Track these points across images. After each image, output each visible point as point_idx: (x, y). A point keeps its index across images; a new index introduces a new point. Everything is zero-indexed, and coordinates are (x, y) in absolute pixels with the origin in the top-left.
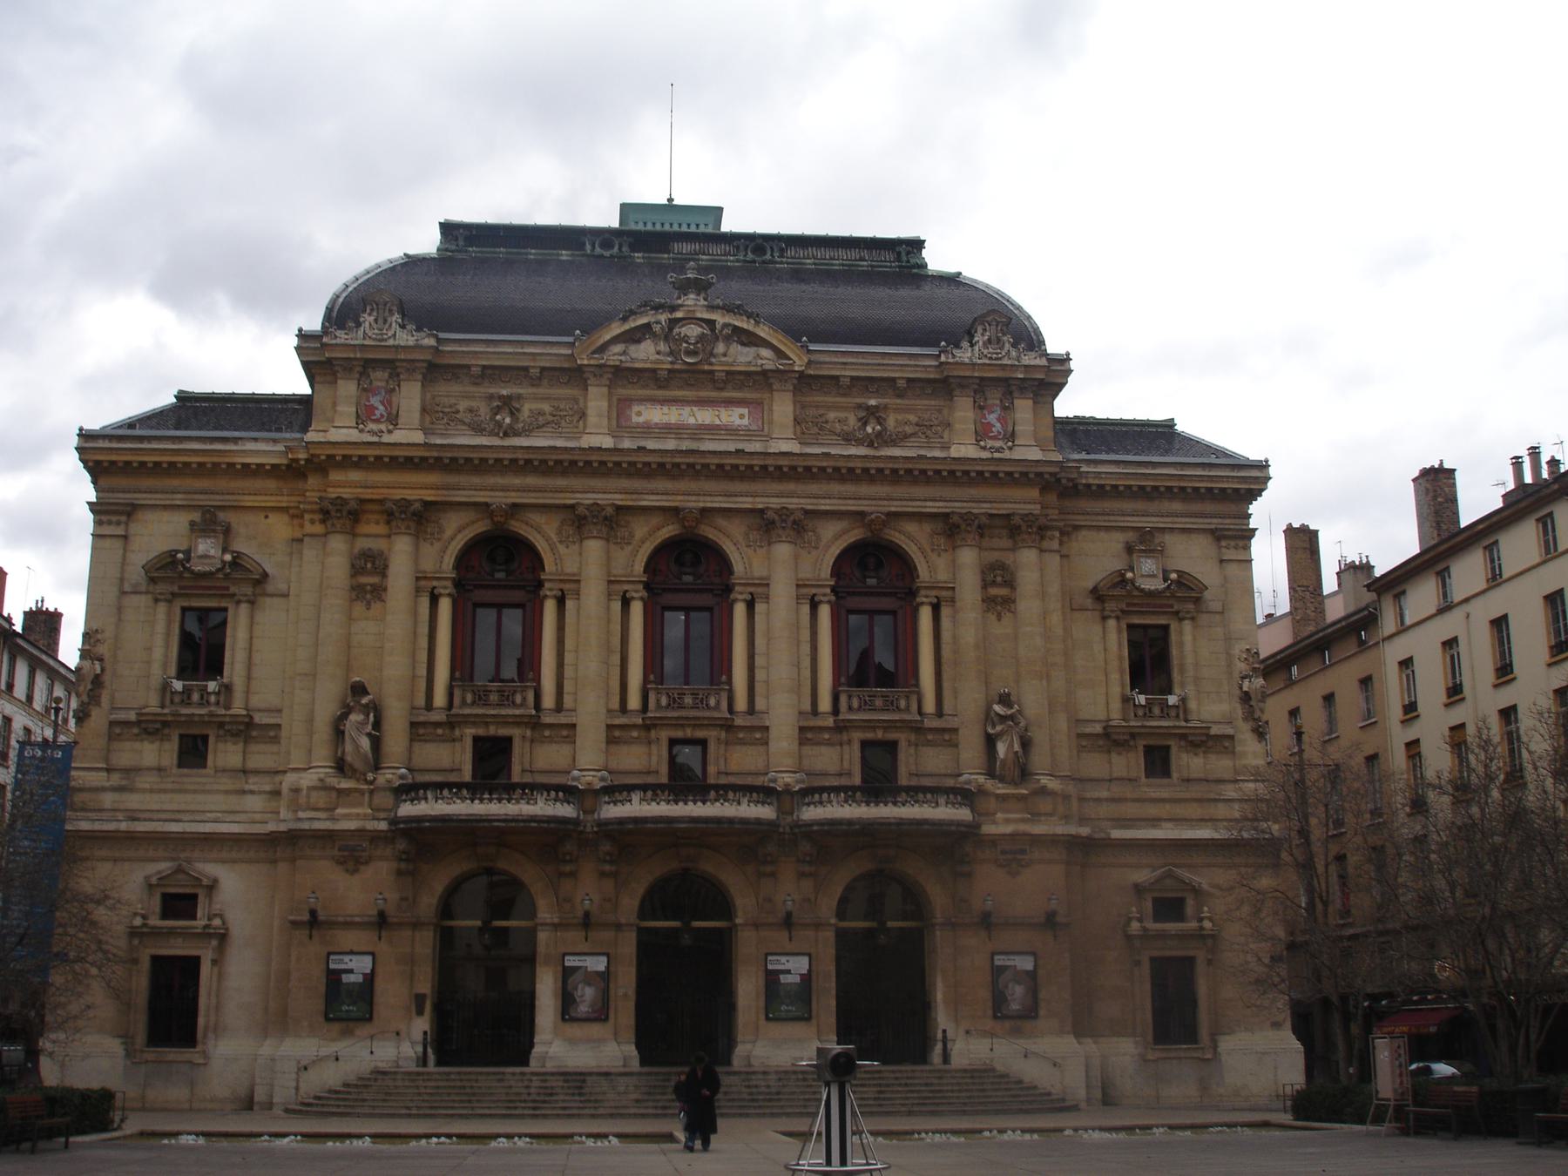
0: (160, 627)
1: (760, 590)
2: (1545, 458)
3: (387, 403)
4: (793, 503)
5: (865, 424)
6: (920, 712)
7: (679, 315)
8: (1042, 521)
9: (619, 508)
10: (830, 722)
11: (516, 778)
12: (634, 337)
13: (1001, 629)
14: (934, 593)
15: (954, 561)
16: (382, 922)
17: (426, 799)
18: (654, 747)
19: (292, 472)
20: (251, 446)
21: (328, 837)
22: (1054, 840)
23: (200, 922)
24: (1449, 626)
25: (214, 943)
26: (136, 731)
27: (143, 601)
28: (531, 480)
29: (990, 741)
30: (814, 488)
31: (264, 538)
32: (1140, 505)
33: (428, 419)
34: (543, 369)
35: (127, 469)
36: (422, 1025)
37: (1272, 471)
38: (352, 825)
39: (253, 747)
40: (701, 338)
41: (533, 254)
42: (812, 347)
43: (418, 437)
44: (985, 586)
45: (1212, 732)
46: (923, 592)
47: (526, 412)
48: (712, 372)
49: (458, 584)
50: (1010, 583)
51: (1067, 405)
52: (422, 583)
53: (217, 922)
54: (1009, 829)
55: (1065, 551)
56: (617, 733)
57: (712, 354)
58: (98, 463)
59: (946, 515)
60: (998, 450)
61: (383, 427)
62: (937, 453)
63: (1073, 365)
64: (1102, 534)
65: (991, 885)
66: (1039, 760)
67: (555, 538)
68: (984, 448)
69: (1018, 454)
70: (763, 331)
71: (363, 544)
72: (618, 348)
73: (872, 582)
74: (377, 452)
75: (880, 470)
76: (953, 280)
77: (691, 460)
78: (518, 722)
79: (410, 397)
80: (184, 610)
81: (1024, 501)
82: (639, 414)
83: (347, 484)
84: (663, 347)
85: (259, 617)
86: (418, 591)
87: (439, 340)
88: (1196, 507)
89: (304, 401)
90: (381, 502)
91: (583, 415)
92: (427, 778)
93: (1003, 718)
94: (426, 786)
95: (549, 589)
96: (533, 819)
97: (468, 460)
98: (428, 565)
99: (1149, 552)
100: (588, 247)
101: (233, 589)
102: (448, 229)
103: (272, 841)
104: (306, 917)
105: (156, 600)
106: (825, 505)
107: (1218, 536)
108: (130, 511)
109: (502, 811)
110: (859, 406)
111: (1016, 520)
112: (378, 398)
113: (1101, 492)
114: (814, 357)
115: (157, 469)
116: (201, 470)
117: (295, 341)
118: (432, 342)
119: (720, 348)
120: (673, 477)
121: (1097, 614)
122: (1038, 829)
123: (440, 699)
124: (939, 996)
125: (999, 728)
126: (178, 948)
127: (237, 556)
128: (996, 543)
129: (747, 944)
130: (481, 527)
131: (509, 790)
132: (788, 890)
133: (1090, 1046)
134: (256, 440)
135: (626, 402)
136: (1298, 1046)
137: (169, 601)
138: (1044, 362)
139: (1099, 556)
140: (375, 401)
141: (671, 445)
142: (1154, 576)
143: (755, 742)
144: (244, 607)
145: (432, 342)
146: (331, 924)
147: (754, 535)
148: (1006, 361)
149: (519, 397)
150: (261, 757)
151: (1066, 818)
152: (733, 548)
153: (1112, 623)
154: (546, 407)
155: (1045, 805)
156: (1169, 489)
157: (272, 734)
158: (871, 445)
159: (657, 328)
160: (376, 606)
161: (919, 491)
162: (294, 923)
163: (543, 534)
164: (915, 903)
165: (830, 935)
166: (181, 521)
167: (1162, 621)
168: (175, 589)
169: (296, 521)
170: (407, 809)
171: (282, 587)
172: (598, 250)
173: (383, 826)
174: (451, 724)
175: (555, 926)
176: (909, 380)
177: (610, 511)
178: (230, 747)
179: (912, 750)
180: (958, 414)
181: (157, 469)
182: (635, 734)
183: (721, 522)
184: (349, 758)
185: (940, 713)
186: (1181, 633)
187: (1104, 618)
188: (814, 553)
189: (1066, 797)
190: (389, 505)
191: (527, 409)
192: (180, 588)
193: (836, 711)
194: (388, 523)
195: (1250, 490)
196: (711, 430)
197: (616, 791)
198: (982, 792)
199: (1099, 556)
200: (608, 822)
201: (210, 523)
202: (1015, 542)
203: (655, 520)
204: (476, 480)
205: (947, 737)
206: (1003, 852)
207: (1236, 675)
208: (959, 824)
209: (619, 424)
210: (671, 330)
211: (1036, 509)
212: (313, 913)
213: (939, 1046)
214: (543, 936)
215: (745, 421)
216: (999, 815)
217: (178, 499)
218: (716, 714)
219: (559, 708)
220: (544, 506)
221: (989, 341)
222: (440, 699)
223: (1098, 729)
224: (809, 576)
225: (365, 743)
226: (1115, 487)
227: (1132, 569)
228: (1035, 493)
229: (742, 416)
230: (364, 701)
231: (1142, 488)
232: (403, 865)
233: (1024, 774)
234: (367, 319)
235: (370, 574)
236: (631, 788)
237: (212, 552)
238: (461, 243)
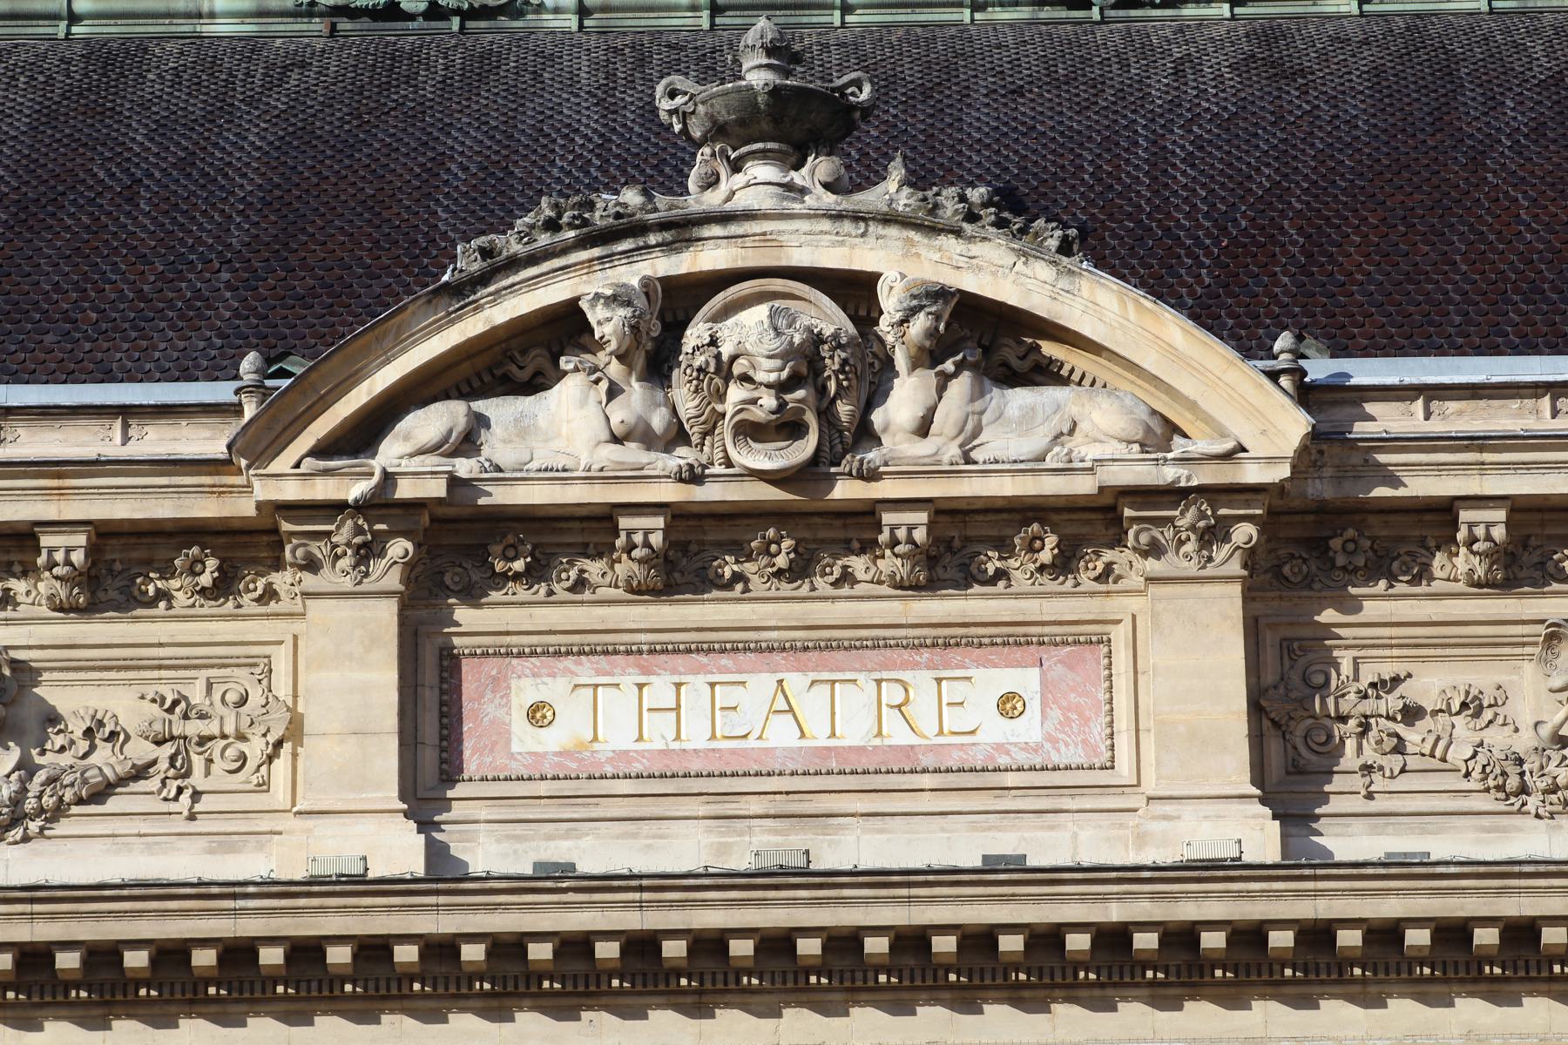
12: (524, 360)
72: (434, 421)
119: (905, 398)
141: (685, 848)
159: (607, 323)
196: (879, 776)
215: (1028, 729)
229: (1009, 705)
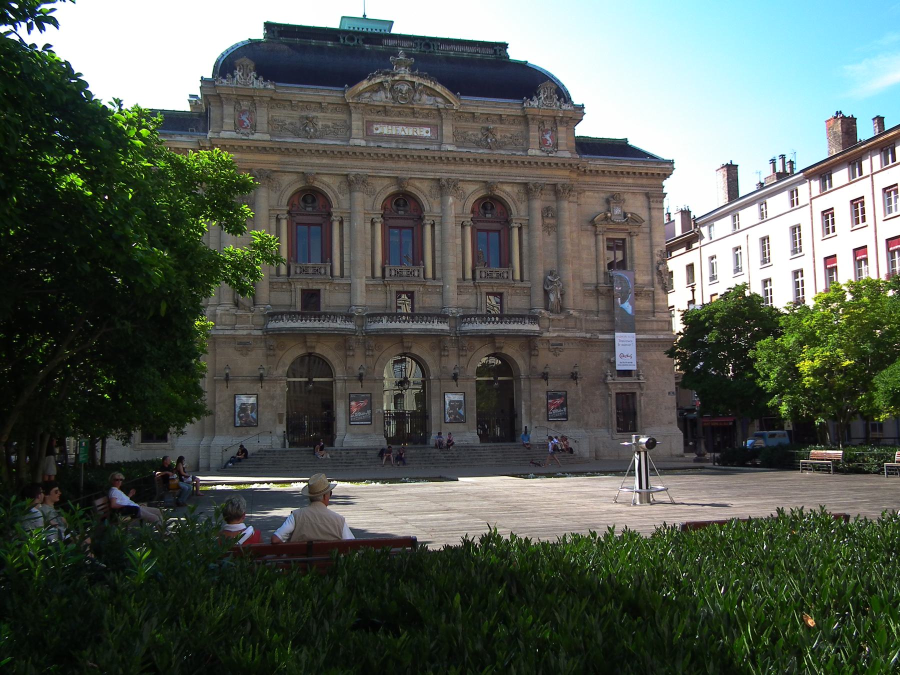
2: (787, 160)
3: (250, 119)
4: (454, 176)
7: (397, 78)
11: (322, 310)
21: (234, 337)
22: (575, 339)
24: (738, 240)
28: (325, 161)
29: (546, 293)
32: (614, 180)
36: (281, 429)
38: (245, 332)
41: (314, 42)
43: (267, 137)
51: (581, 130)
54: (555, 335)
63: (585, 110)
66: (569, 302)
72: (367, 95)
76: (523, 66)
77: (405, 153)
79: (262, 116)
81: (561, 176)
82: (377, 129)
88: (639, 181)
91: (349, 128)
96: (336, 329)
100: (342, 40)
102: (268, 26)
117: (200, 84)
118: (273, 87)
119: (417, 96)
122: (568, 335)
124: (523, 411)
125: (550, 287)
131: (319, 316)
135: (369, 125)
136: (680, 433)
139: (593, 203)
151: (581, 330)
154: (330, 124)
155: (571, 323)
159: (386, 85)
161: (514, 171)
162: (215, 380)
170: (273, 325)
172: (347, 42)
173: (260, 333)
175: (345, 380)
180: (531, 134)
188: (463, 201)
191: (320, 123)
193: (474, 278)
197: (374, 316)
208: (534, 331)
209: (368, 134)
211: (567, 181)
214: (339, 385)
215: (429, 135)
220: (331, 174)
228: (567, 173)
229: (427, 132)
232: (272, 352)
233: (562, 309)
234: (238, 73)
236: (381, 315)
238: (276, 34)
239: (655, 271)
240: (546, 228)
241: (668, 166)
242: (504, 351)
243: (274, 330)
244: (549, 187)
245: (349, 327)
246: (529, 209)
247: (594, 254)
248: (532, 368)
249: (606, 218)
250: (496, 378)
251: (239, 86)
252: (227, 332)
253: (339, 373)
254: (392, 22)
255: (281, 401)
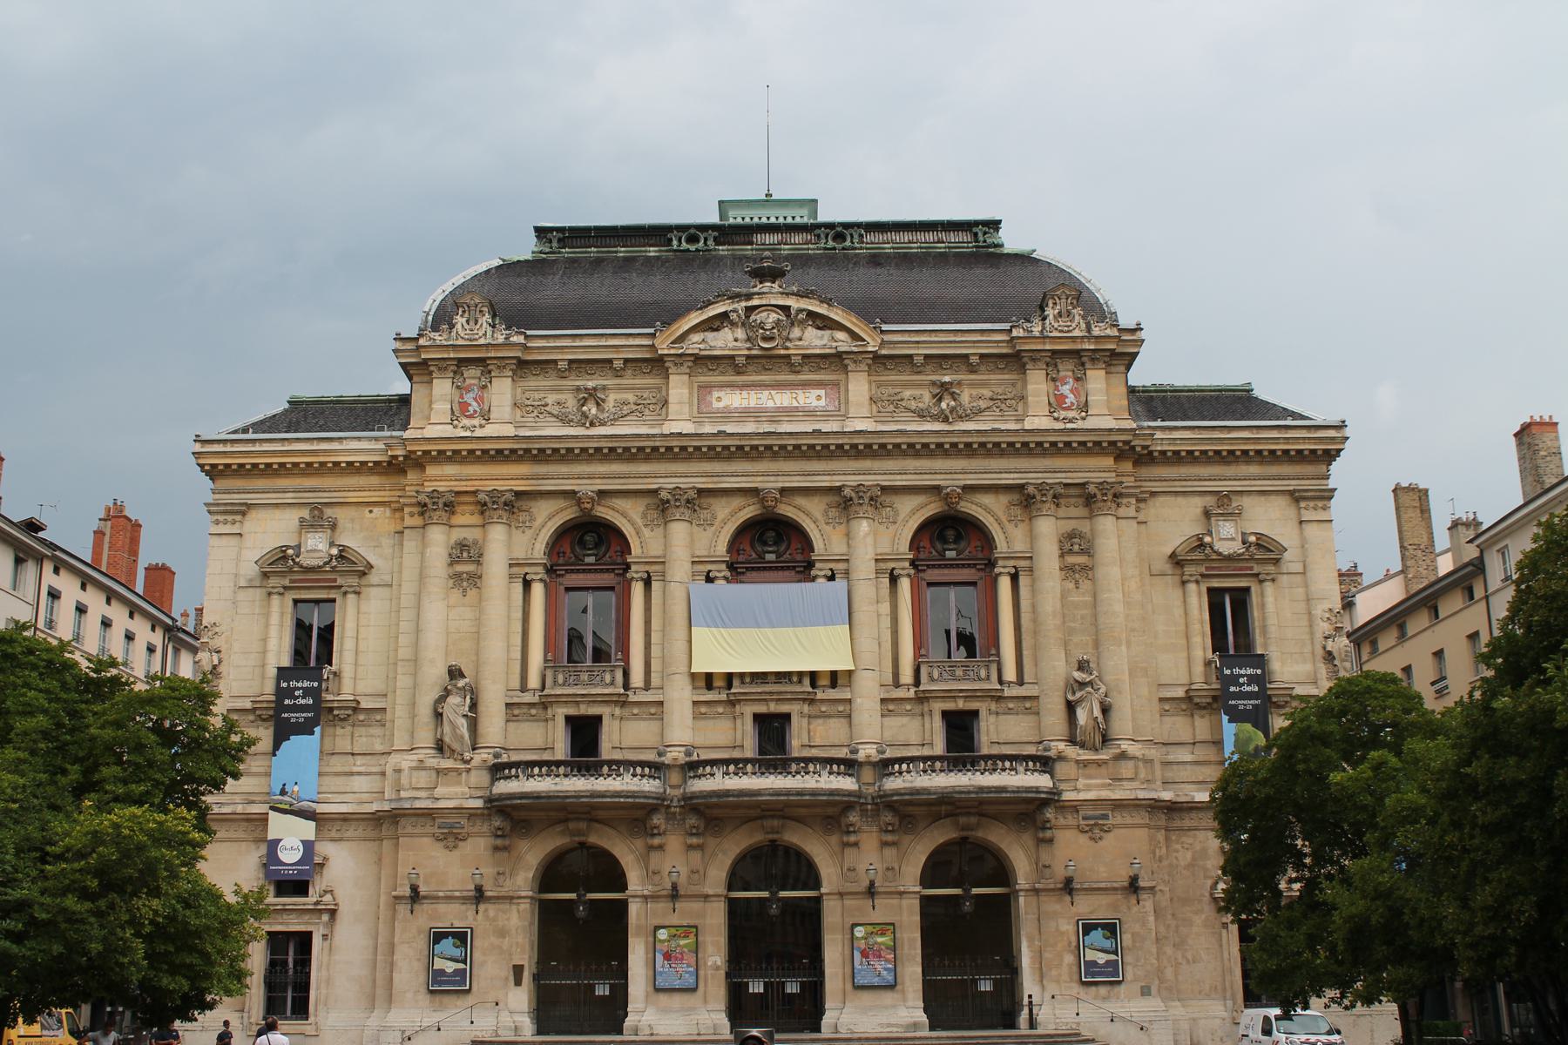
0: (275, 619)
1: (842, 566)
5: (940, 400)
6: (1001, 682)
7: (755, 302)
8: (1118, 489)
9: (700, 492)
10: (911, 694)
13: (1080, 597)
14: (1012, 563)
15: (1031, 531)
16: (479, 896)
17: (517, 777)
18: (739, 722)
19: (393, 468)
20: (335, 446)
21: (429, 814)
23: (312, 898)
25: (325, 917)
26: (251, 717)
27: (258, 594)
28: (616, 468)
29: (1071, 707)
30: (890, 464)
31: (364, 533)
33: (519, 413)
34: (626, 361)
35: (241, 471)
37: (1347, 432)
38: (451, 804)
39: (362, 730)
40: (778, 323)
41: (622, 252)
42: (885, 327)
43: (509, 431)
44: (1062, 556)
45: (1295, 692)
46: (1000, 563)
47: (610, 404)
48: (788, 356)
49: (551, 570)
50: (1087, 552)
52: (515, 570)
53: (328, 898)
55: (1141, 517)
56: (703, 710)
57: (788, 339)
58: (214, 466)
59: (1021, 487)
60: (1071, 421)
61: (476, 422)
62: (1012, 426)
64: (1180, 500)
65: (1070, 849)
66: (1122, 725)
67: (639, 521)
68: (1056, 419)
69: (1091, 423)
70: (837, 315)
71: (458, 534)
72: (696, 337)
73: (950, 554)
74: (470, 447)
75: (953, 445)
78: (607, 700)
80: (296, 602)
81: (1098, 469)
83: (442, 478)
84: (740, 333)
85: (364, 608)
86: (511, 576)
87: (527, 337)
88: (1274, 470)
89: (405, 400)
90: (475, 493)
92: (515, 757)
93: (1082, 685)
94: (517, 765)
95: (636, 571)
97: (555, 450)
98: (520, 553)
99: (1228, 516)
100: (675, 242)
101: (340, 581)
103: (377, 819)
104: (407, 892)
105: (270, 594)
106: (900, 481)
107: (1296, 497)
108: (243, 510)
109: (589, 787)
110: (934, 383)
111: (1092, 489)
112: (471, 395)
113: (1176, 458)
114: (887, 338)
115: (269, 471)
116: (309, 470)
118: (521, 339)
119: (796, 332)
120: (753, 459)
121: (1177, 578)
122: (1117, 795)
123: (534, 681)
125: (1078, 695)
126: (295, 925)
127: (343, 549)
128: (1074, 512)
129: (832, 915)
130: (569, 514)
132: (869, 857)
133: (1177, 1010)
134: (359, 439)
135: (706, 388)
137: (281, 594)
138: (1115, 332)
139: (1175, 521)
140: (469, 398)
141: (749, 428)
142: (1233, 539)
143: (840, 715)
144: (350, 596)
145: (521, 339)
146: (435, 899)
147: (833, 513)
148: (1076, 333)
149: (604, 388)
150: (368, 738)
152: (813, 526)
153: (1192, 587)
154: (631, 397)
155: (1126, 769)
156: (1245, 452)
157: (378, 717)
158: (946, 420)
159: (733, 316)
160: (472, 593)
161: (994, 463)
162: (396, 898)
163: (627, 517)
164: (1002, 873)
165: (916, 903)
166: (291, 518)
167: (1242, 583)
168: (286, 582)
169: (398, 515)
171: (387, 578)
172: (684, 245)
173: (479, 803)
174: (544, 705)
175: (645, 897)
176: (982, 356)
177: (692, 494)
178: (339, 731)
179: (992, 719)
181: (269, 471)
182: (721, 710)
183: (800, 501)
184: (447, 739)
185: (1020, 681)
186: (1262, 595)
187: (1184, 583)
188: (892, 528)
189: (1148, 762)
190: (482, 496)
191: (612, 399)
192: (292, 581)
193: (917, 683)
194: (482, 513)
195: (1326, 452)
196: (790, 412)
198: (1061, 758)
199: (1175, 521)
200: (694, 796)
201: (318, 518)
202: (1091, 511)
203: (737, 502)
204: (564, 469)
205: (1028, 705)
206: (1084, 818)
207: (1319, 636)
209: (702, 411)
210: (748, 317)
211: (1111, 477)
212: (414, 889)
213: (1026, 1011)
214: (634, 909)
215: (822, 403)
216: (1081, 782)
217: (289, 498)
218: (798, 688)
219: (647, 686)
221: (1060, 315)
222: (534, 681)
223: (1180, 693)
224: (887, 550)
225: (463, 724)
226: (1190, 453)
227: (1210, 533)
228: (1109, 462)
230: (461, 683)
231: (1217, 452)
232: (499, 842)
233: (1106, 740)
234: (460, 320)
235: (465, 562)
237: (320, 547)
238: (555, 244)
239: (1319, 652)
240: (1068, 570)
241: (1332, 433)
242: (980, 834)
243: (502, 797)
244: (1072, 491)
245: (647, 788)
246: (1032, 537)
247: (1182, 621)
248: (1042, 869)
249: (1201, 545)
250: (967, 891)
251: (460, 342)
252: (418, 804)
253: (635, 882)
254: (720, 203)
255: (520, 940)
